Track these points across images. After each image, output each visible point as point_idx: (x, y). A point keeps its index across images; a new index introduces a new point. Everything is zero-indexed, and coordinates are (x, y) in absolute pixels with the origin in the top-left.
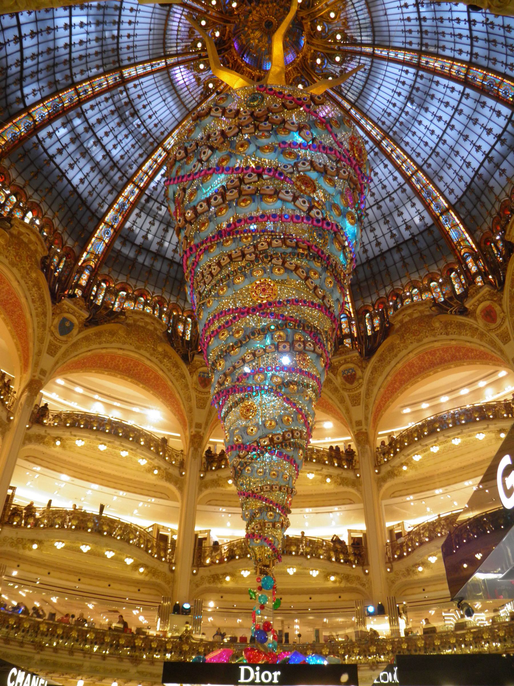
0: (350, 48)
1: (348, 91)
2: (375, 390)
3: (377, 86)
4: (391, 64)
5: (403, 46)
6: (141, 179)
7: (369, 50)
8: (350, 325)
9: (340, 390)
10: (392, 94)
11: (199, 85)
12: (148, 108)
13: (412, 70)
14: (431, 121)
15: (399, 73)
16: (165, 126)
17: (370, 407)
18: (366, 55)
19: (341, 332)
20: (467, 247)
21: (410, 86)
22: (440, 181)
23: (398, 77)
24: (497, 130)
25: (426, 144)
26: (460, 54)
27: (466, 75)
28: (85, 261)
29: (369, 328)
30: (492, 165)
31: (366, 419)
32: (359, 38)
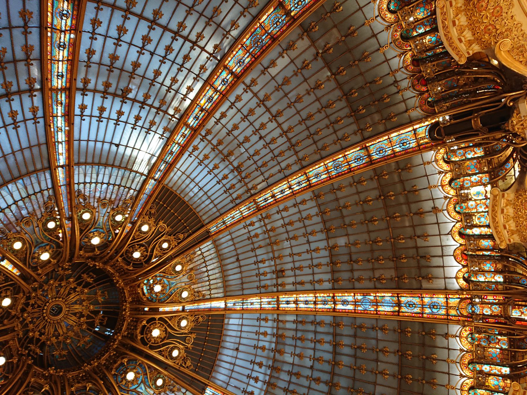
0: (65, 204)
1: (130, 188)
3: (114, 148)
4: (76, 136)
5: (41, 121)
7: (61, 174)
10: (122, 125)
13: (78, 99)
14: (152, 54)
15: (87, 119)
18: (69, 176)
21: (104, 98)
23: (94, 120)
32: (46, 193)
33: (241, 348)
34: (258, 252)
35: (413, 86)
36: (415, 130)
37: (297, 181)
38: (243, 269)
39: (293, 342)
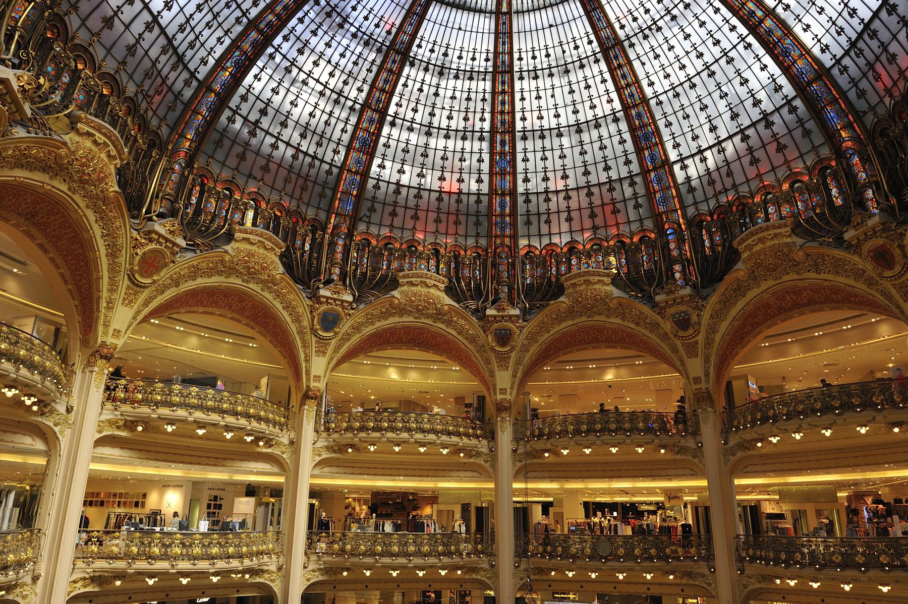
2: (718, 337)
8: (681, 241)
9: (672, 336)
16: (390, 22)
17: (712, 359)
29: (707, 243)
30: (894, 18)
31: (707, 374)
33: (462, 33)
34: (559, 50)
35: (720, 206)
36: (676, 211)
37: (635, 93)
38: (541, 32)
39: (466, 89)
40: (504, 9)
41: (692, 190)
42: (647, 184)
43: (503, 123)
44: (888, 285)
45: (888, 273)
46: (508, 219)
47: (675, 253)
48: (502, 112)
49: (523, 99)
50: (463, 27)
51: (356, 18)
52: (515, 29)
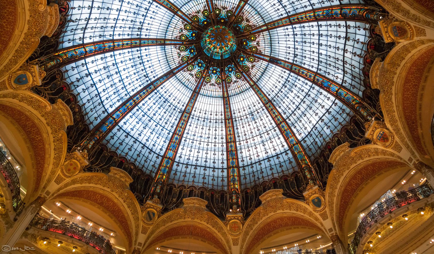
3: (277, 42)
6: (180, 131)
8: (310, 172)
9: (314, 212)
11: (193, 77)
12: (172, 96)
19: (307, 177)
20: (356, 104)
22: (329, 75)
24: (343, 35)
25: (313, 59)
26: (306, 8)
27: (314, 15)
28: (158, 179)
32: (258, 24)
40: (226, 95)
41: (310, 149)
42: (293, 153)
43: (231, 138)
44: (390, 150)
45: (387, 144)
46: (236, 177)
47: (309, 176)
48: (230, 134)
49: (237, 129)
50: (211, 103)
51: (171, 100)
52: (231, 103)
